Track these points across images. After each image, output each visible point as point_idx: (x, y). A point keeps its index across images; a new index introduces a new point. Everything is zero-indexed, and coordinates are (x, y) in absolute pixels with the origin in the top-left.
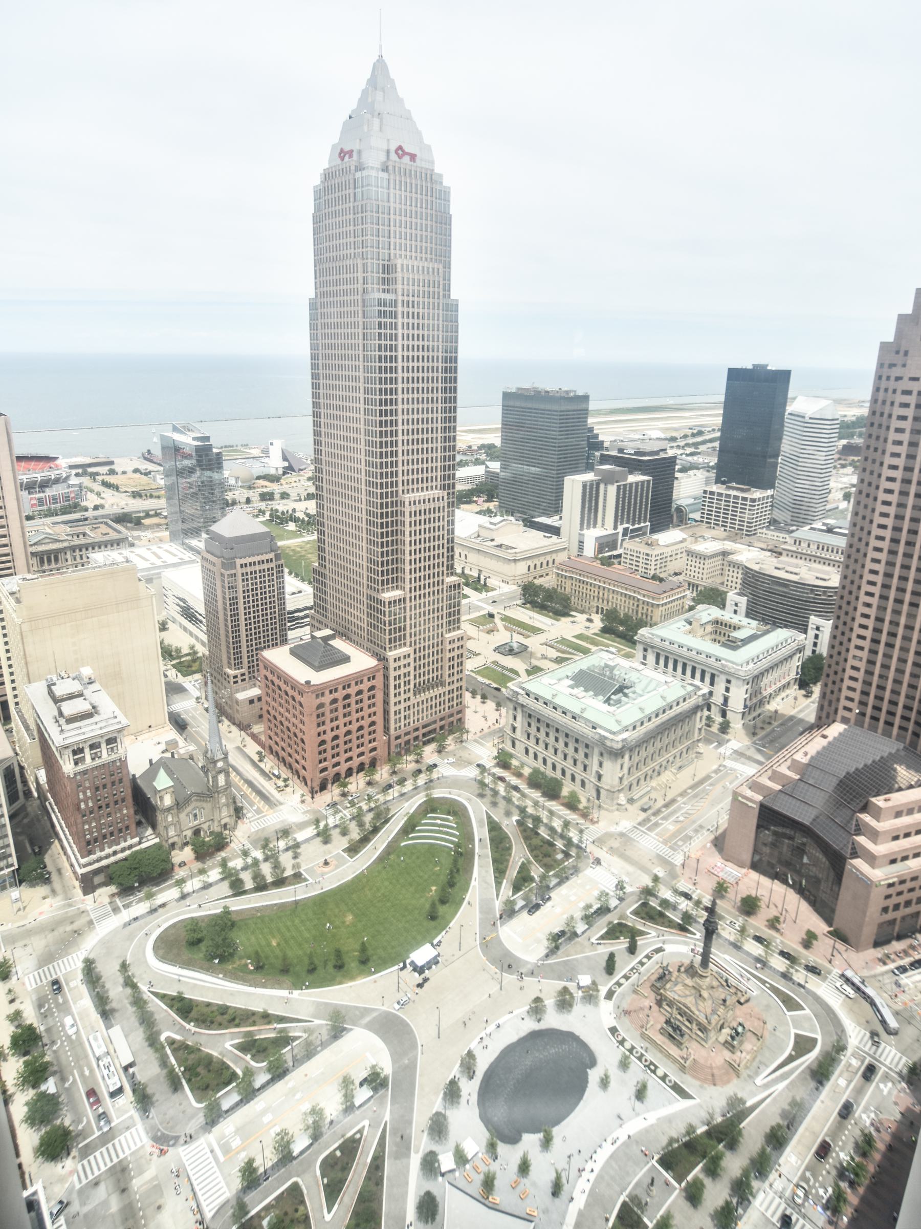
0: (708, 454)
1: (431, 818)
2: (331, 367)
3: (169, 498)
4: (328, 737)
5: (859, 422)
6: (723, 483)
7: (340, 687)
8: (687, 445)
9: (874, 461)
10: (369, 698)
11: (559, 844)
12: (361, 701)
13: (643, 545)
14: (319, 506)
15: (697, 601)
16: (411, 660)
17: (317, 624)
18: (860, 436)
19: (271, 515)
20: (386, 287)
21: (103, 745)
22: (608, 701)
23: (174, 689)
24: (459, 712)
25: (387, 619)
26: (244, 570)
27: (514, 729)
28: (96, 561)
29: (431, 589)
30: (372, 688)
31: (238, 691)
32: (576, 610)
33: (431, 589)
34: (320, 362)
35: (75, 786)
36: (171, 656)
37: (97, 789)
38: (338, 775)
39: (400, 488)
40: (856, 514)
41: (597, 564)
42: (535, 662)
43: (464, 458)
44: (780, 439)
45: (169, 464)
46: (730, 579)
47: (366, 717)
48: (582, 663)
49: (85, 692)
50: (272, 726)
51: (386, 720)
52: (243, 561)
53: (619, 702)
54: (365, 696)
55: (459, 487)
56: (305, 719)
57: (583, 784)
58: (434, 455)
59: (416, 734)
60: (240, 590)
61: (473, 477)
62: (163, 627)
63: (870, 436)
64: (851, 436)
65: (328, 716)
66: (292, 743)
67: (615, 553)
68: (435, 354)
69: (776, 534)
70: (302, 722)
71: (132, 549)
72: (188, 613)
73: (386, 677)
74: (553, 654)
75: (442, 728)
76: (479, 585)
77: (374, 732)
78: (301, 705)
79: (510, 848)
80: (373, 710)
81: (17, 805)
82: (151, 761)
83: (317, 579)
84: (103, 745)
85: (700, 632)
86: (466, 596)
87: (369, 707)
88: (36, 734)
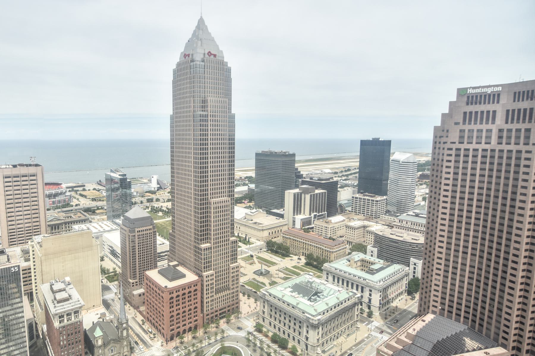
0: (353, 180)
2: (179, 144)
3: (107, 201)
4: (175, 314)
5: (427, 163)
6: (362, 193)
7: (181, 289)
8: (343, 175)
9: (436, 182)
10: (194, 295)
12: (191, 296)
13: (324, 223)
15: (352, 250)
16: (214, 277)
17: (171, 259)
18: (428, 170)
19: (151, 209)
21: (73, 314)
23: (105, 288)
24: (237, 303)
25: (203, 257)
27: (264, 312)
28: (75, 229)
29: (224, 243)
30: (196, 290)
32: (292, 254)
33: (224, 243)
35: (59, 333)
36: (105, 273)
37: (69, 335)
38: (179, 333)
39: (209, 196)
40: (430, 207)
41: (302, 232)
42: (273, 279)
43: (238, 183)
44: (388, 172)
45: (108, 186)
46: (368, 239)
47: (193, 304)
48: (297, 280)
49: (67, 289)
50: (149, 307)
51: (202, 306)
54: (192, 294)
55: (236, 196)
56: (164, 305)
59: (216, 313)
60: (137, 242)
63: (433, 170)
64: (424, 170)
65: (175, 303)
66: (158, 316)
67: (310, 226)
69: (390, 217)
70: (163, 306)
71: (91, 224)
72: (113, 253)
73: (202, 285)
74: (282, 275)
75: (229, 311)
76: (246, 241)
77: (196, 312)
80: (196, 301)
81: (33, 341)
82: (93, 322)
83: (171, 238)
84: (73, 314)
85: (355, 265)
87: (194, 299)
88: (43, 308)
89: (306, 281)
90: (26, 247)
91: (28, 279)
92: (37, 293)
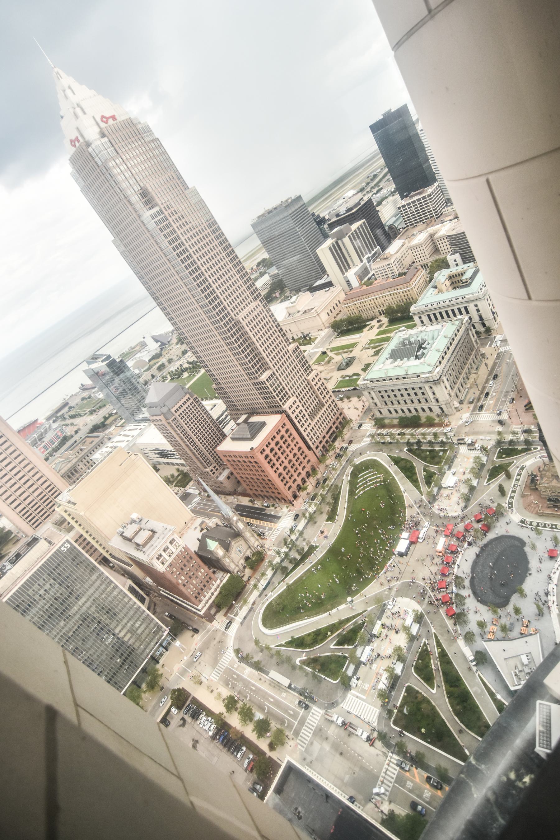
1: (361, 477)
4: (281, 470)
10: (289, 437)
11: (437, 448)
14: (195, 353)
16: (298, 403)
17: (236, 417)
20: (150, 206)
22: (417, 357)
23: (185, 497)
24: (341, 414)
25: (271, 389)
26: (179, 413)
30: (287, 431)
31: (217, 477)
34: (142, 273)
38: (298, 485)
39: (232, 314)
47: (294, 447)
49: (142, 526)
52: (175, 408)
53: (423, 354)
57: (431, 410)
58: (239, 284)
59: (325, 439)
61: (264, 284)
62: (157, 470)
65: (274, 459)
68: (202, 226)
70: (263, 471)
75: (337, 428)
77: (303, 452)
78: (256, 463)
79: (413, 468)
80: (295, 442)
82: (198, 539)
86: (305, 351)
87: (292, 441)
88: (131, 562)
89: (402, 340)
90: (55, 517)
91: (88, 547)
92: (110, 554)
